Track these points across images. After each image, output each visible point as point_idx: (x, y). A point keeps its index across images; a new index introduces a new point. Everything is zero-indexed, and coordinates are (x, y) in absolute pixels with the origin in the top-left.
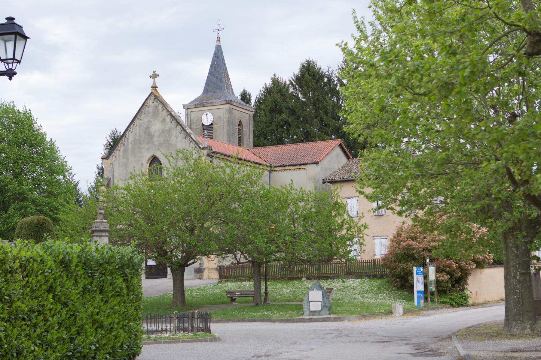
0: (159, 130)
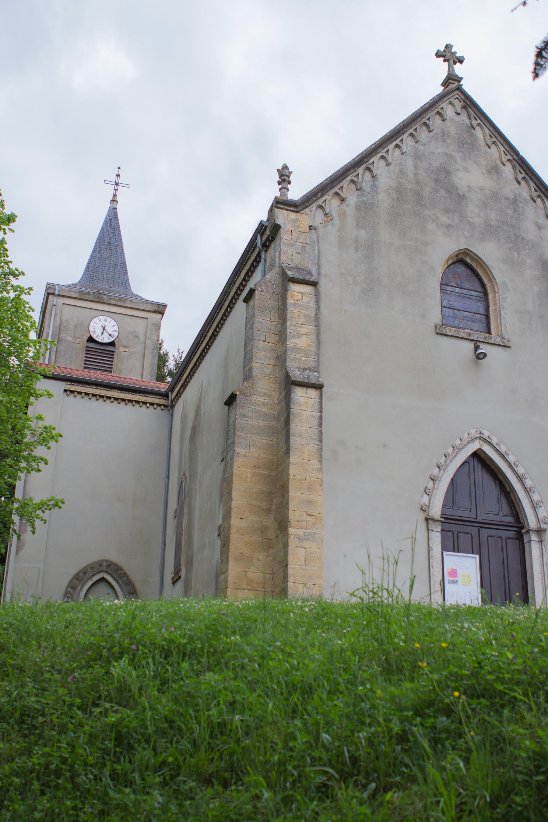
0: (482, 189)
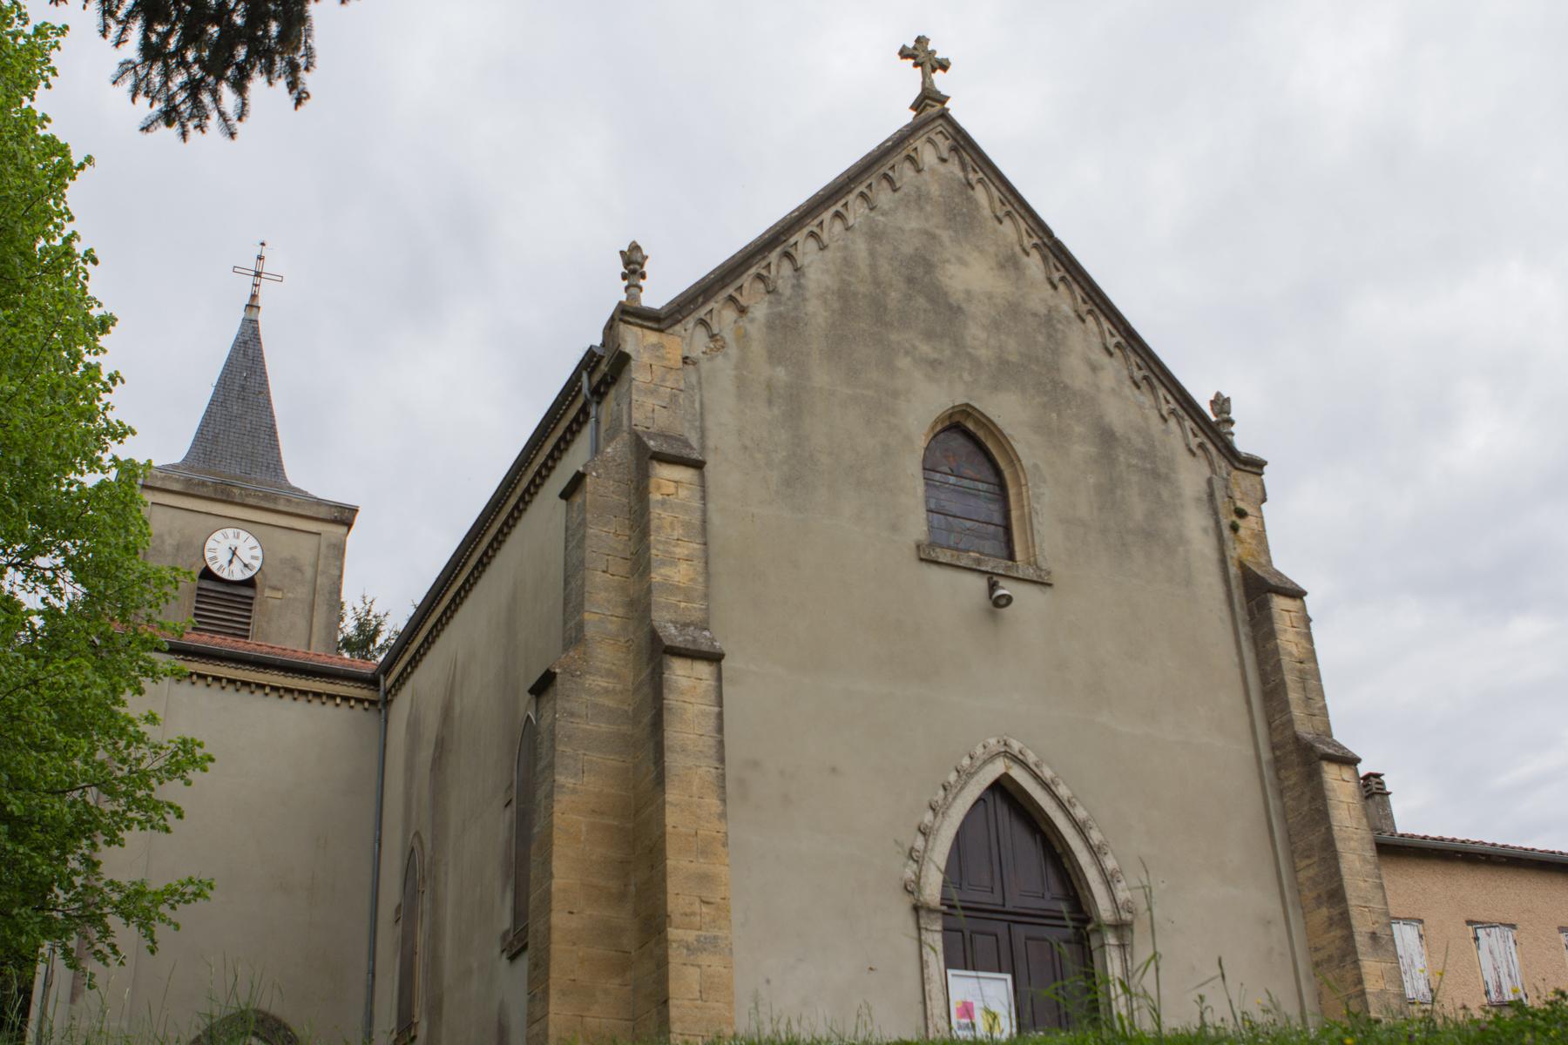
0: (990, 297)
